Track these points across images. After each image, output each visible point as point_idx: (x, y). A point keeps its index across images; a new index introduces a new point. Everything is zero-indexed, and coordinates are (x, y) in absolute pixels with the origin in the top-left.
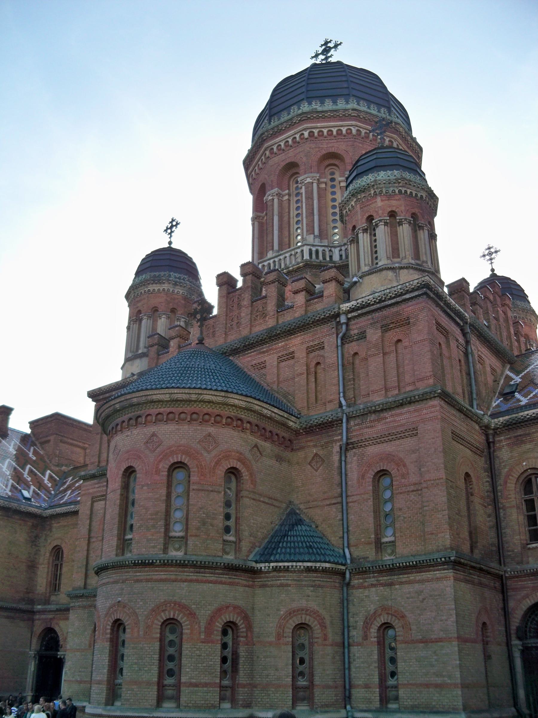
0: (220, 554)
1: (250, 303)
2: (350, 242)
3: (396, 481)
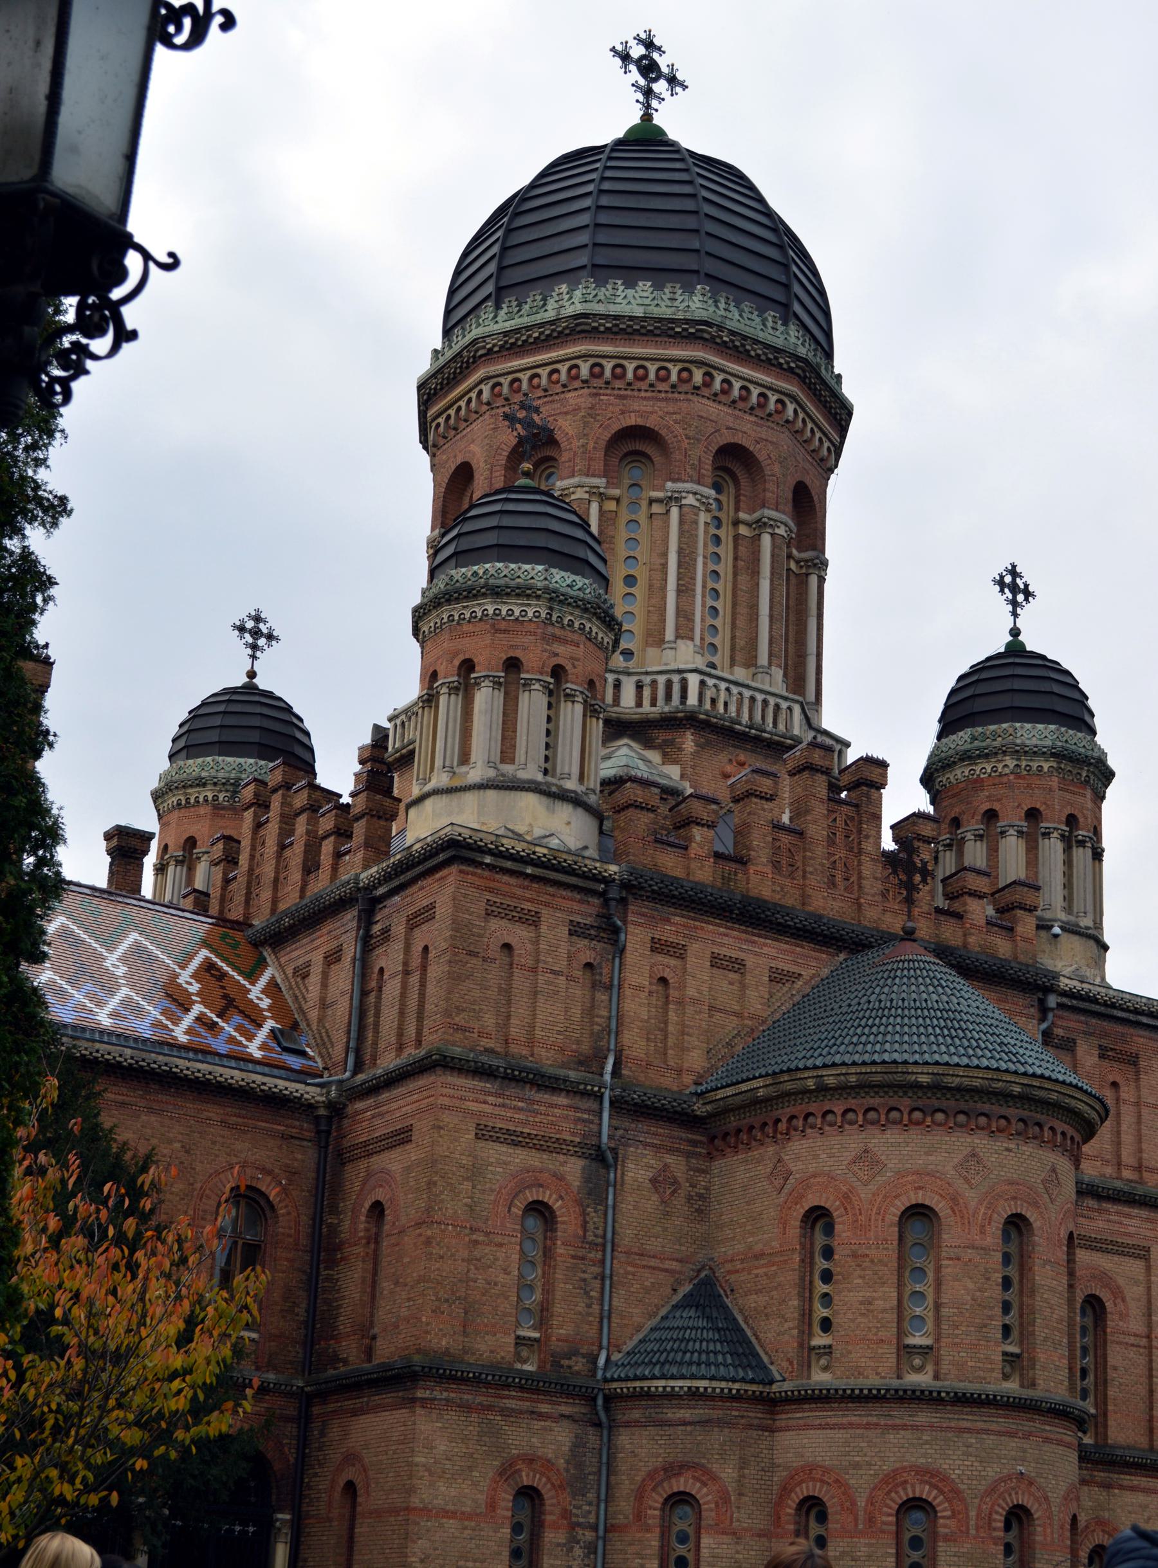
3: (1113, 1321)
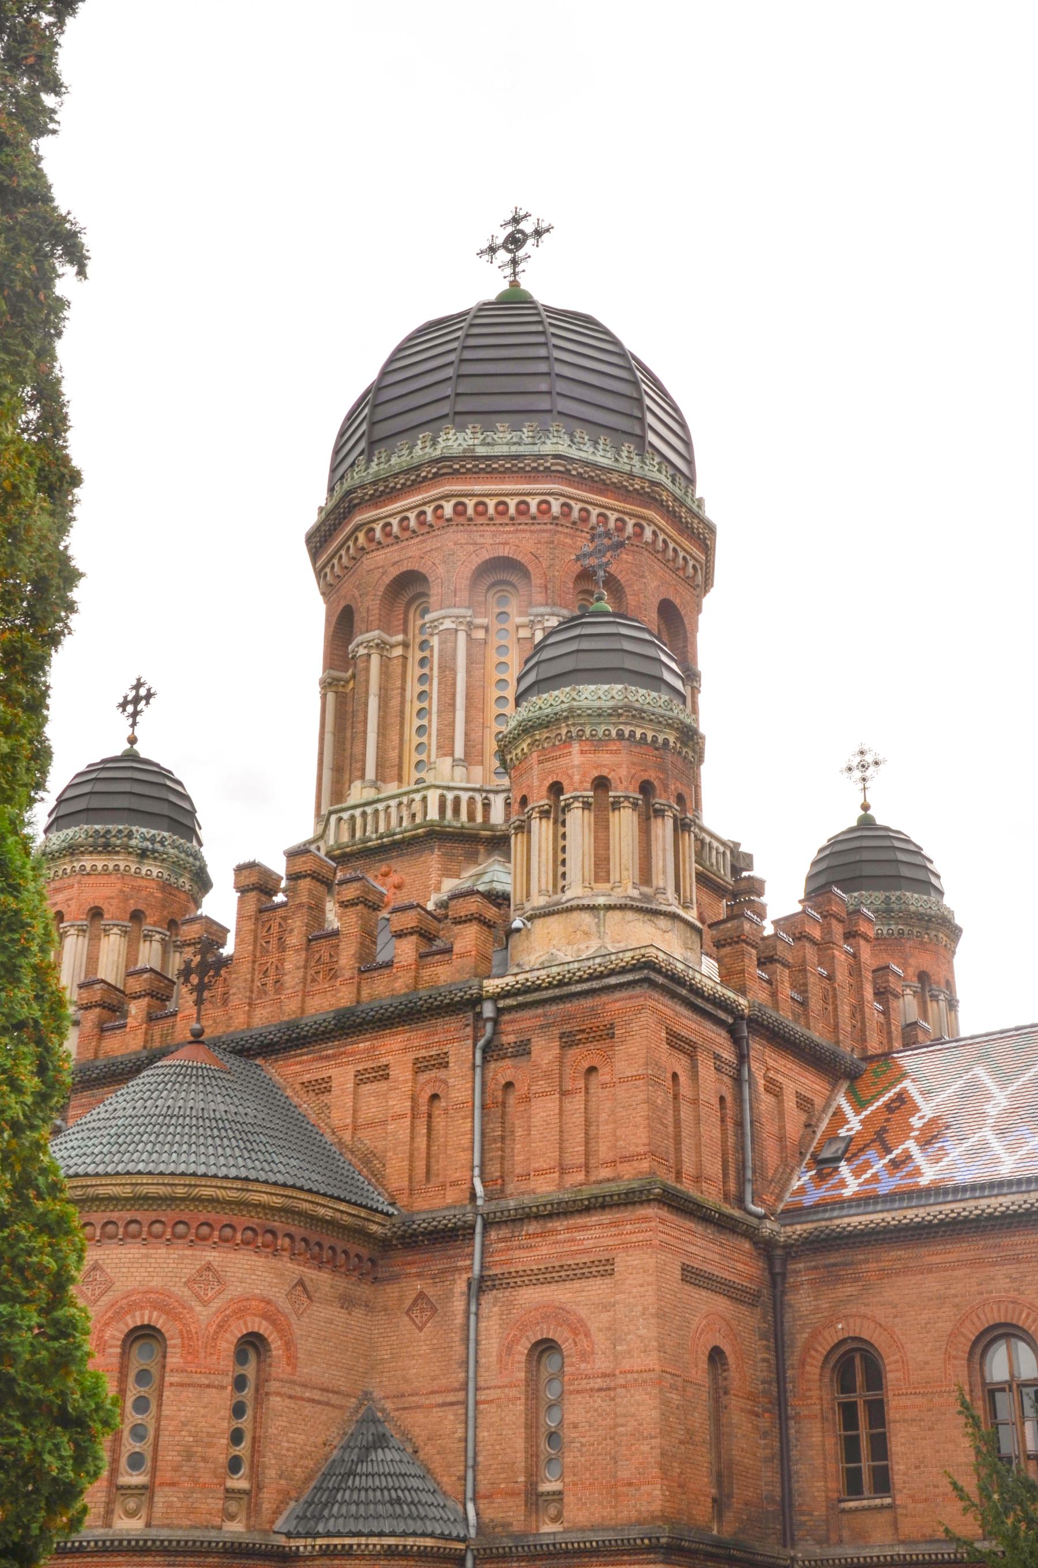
0: (217, 1521)
1: (304, 940)
2: (515, 828)
3: (572, 1365)
